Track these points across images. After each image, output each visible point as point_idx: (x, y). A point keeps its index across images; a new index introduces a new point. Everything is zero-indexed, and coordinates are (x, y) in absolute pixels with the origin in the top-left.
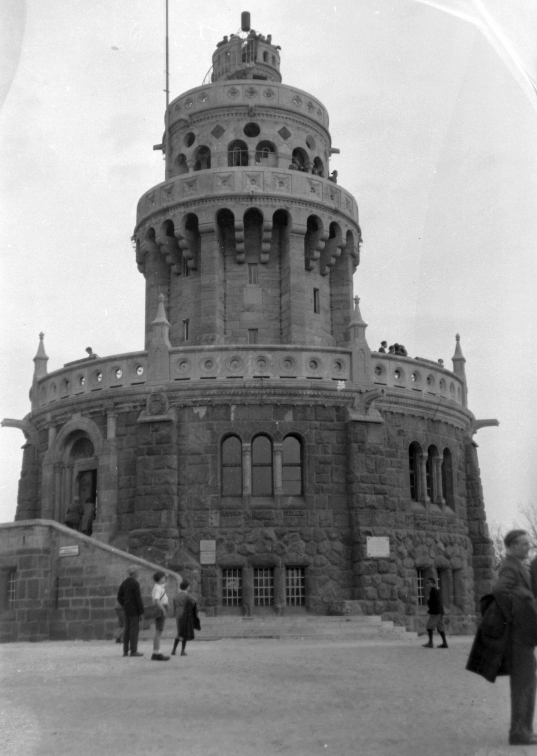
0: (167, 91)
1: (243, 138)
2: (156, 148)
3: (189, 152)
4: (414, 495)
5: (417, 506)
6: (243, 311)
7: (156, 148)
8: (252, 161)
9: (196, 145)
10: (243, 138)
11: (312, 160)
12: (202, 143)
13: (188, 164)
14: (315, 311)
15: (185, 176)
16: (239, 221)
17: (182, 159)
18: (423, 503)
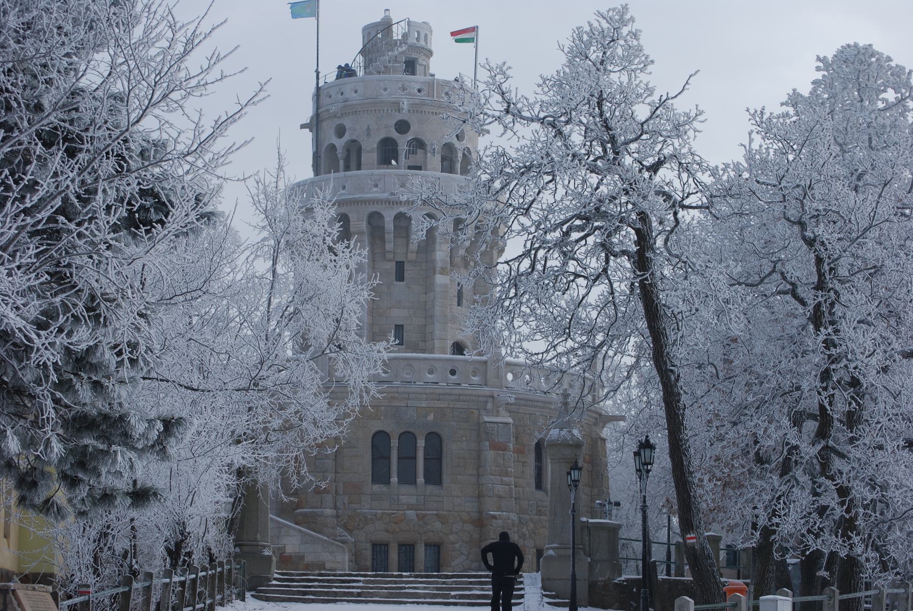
0: (318, 73)
1: (395, 135)
2: (303, 126)
3: (340, 143)
4: (539, 485)
5: (540, 494)
6: (390, 308)
7: (303, 126)
8: (402, 158)
9: (347, 137)
10: (395, 135)
11: (460, 155)
12: (354, 138)
13: (339, 156)
14: (459, 304)
15: (337, 174)
16: (389, 224)
17: (333, 147)
18: (546, 491)
